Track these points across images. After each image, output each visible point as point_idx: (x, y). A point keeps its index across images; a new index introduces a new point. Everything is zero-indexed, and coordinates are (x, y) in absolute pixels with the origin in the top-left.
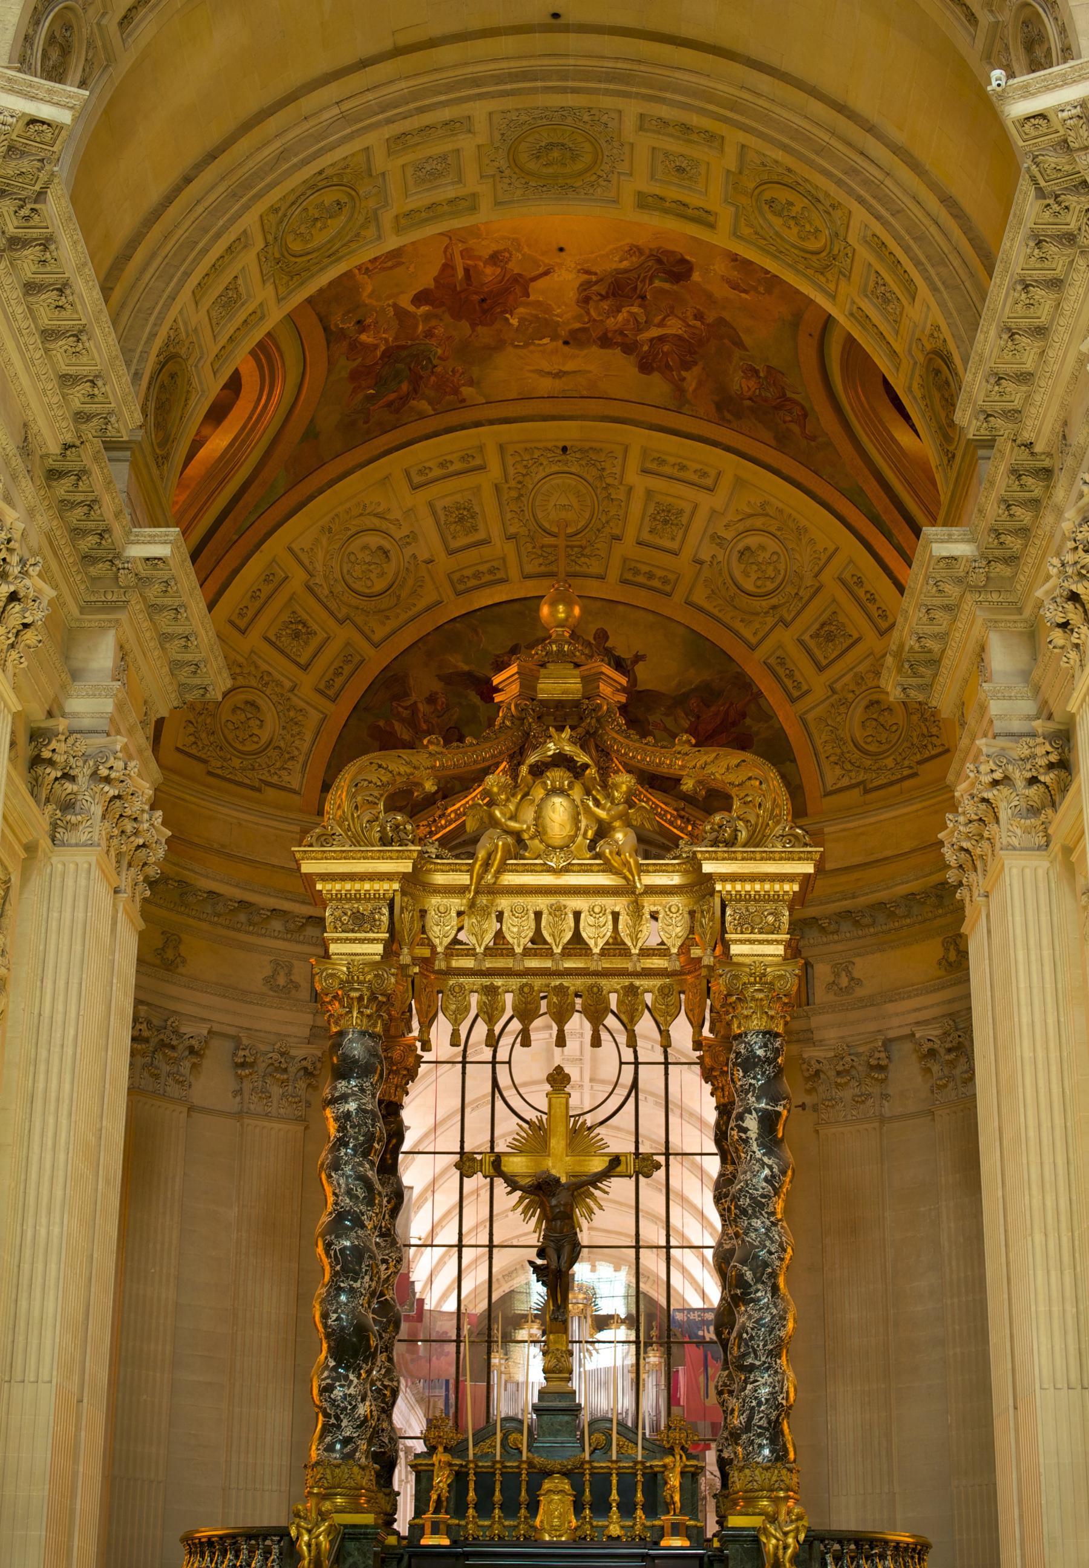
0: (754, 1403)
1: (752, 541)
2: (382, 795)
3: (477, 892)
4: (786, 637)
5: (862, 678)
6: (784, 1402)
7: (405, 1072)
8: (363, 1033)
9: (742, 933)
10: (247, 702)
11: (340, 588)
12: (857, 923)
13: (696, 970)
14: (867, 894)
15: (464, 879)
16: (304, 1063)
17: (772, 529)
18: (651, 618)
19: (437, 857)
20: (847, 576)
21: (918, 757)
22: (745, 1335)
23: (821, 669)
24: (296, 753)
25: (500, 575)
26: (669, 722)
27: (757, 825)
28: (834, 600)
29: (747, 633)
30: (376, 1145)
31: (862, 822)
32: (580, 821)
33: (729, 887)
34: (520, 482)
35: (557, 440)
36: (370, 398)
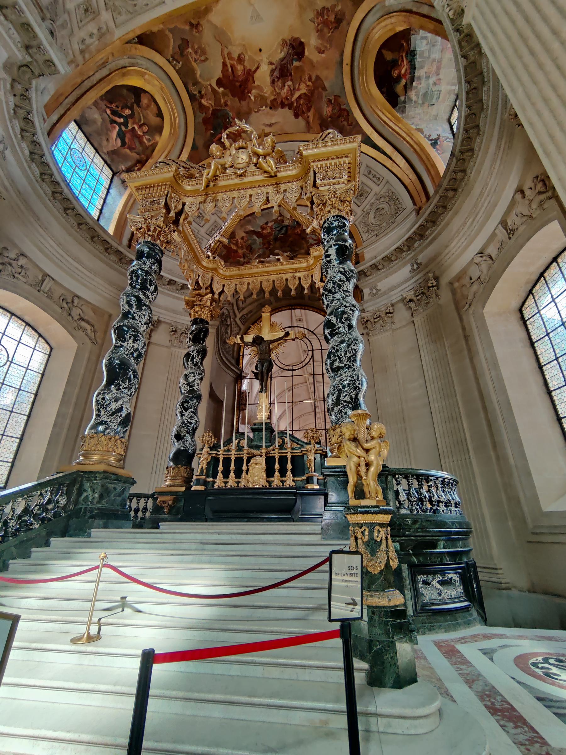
0: (341, 387)
6: (360, 386)
22: (333, 351)
23: (359, 206)
30: (148, 286)
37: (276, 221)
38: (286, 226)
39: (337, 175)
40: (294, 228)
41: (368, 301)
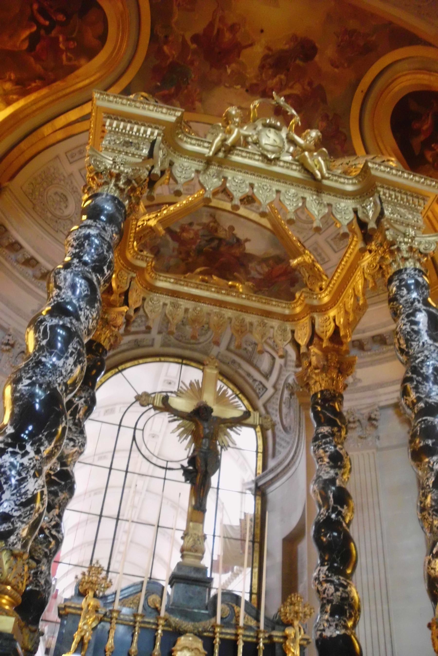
8: (114, 199)
10: (62, 194)
26: (259, 268)
30: (105, 268)
32: (284, 145)
37: (206, 226)
38: (221, 240)
40: (231, 246)
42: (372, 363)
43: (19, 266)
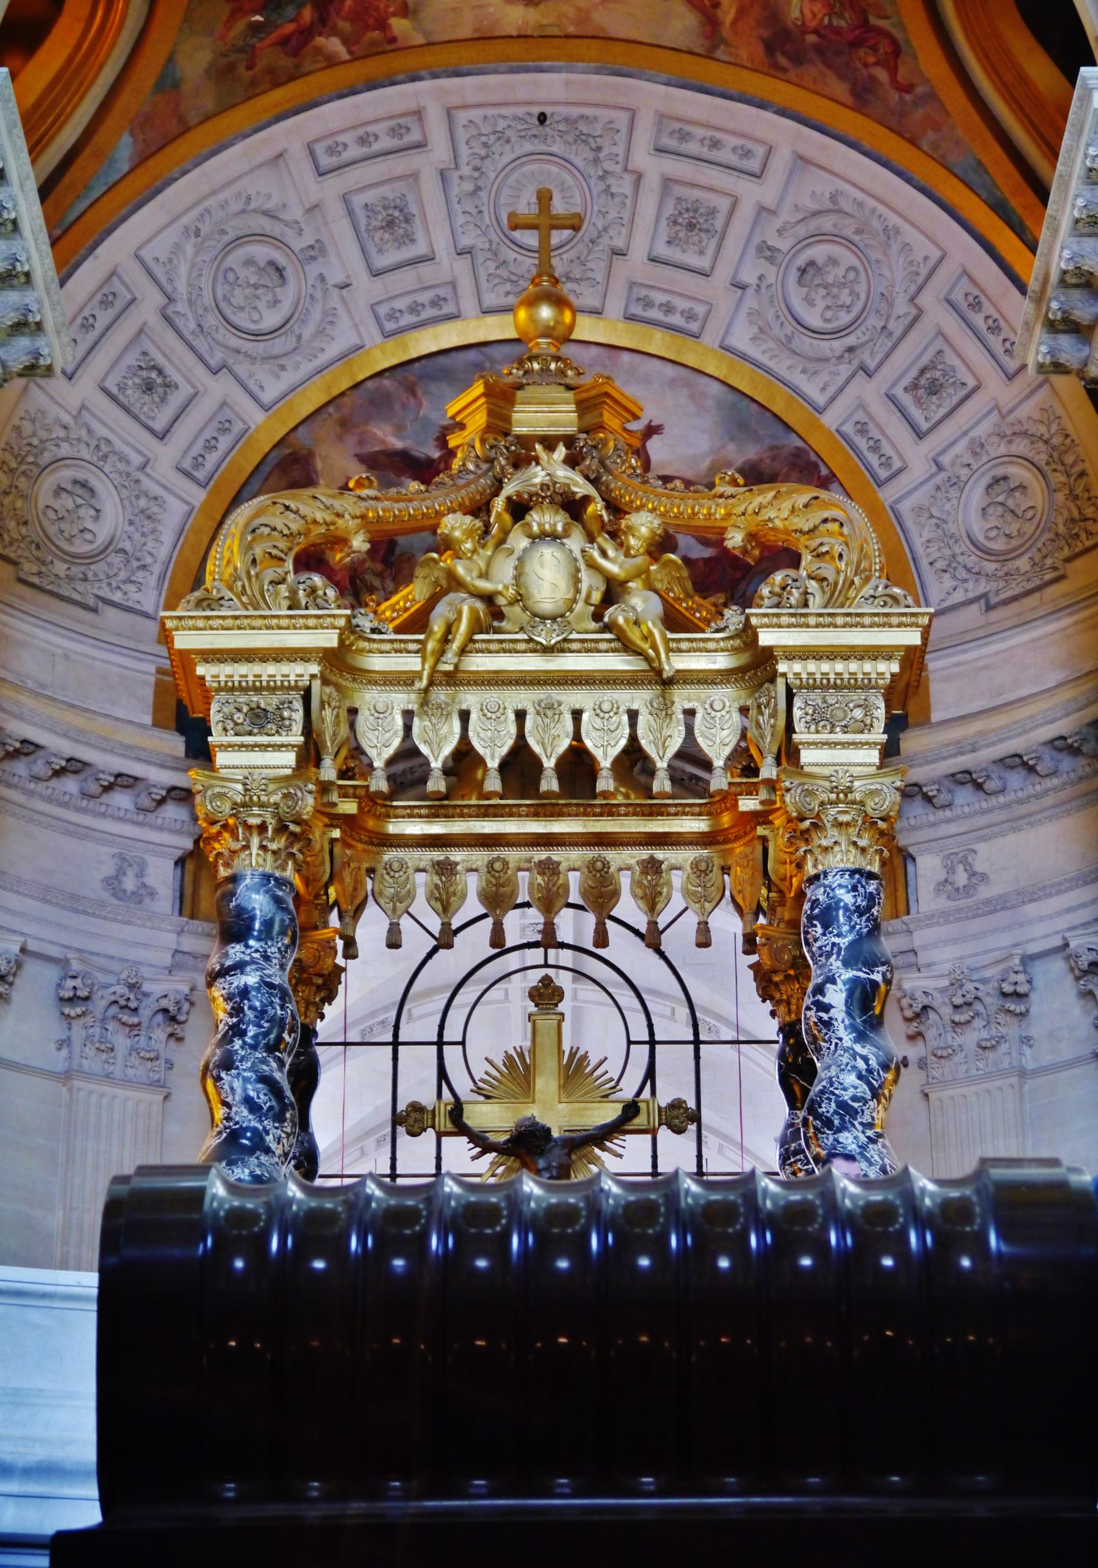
1: (819, 252)
2: (290, 549)
3: (431, 683)
4: (870, 391)
5: (982, 445)
7: (320, 981)
8: (267, 877)
9: (817, 732)
10: (75, 482)
11: (212, 320)
12: (979, 787)
13: (746, 834)
14: (994, 744)
15: (412, 663)
16: (164, 1003)
17: (849, 232)
18: (670, 370)
19: (374, 631)
20: (958, 296)
21: (1066, 552)
23: (920, 435)
24: (149, 560)
25: (448, 308)
27: (836, 584)
28: (940, 333)
29: (812, 390)
30: (286, 1036)
31: (984, 651)
33: (797, 667)
34: (476, 169)
35: (531, 103)
36: (255, 28)
39: (858, 713)
41: (932, 919)
42: (1015, 824)
43: (40, 787)
